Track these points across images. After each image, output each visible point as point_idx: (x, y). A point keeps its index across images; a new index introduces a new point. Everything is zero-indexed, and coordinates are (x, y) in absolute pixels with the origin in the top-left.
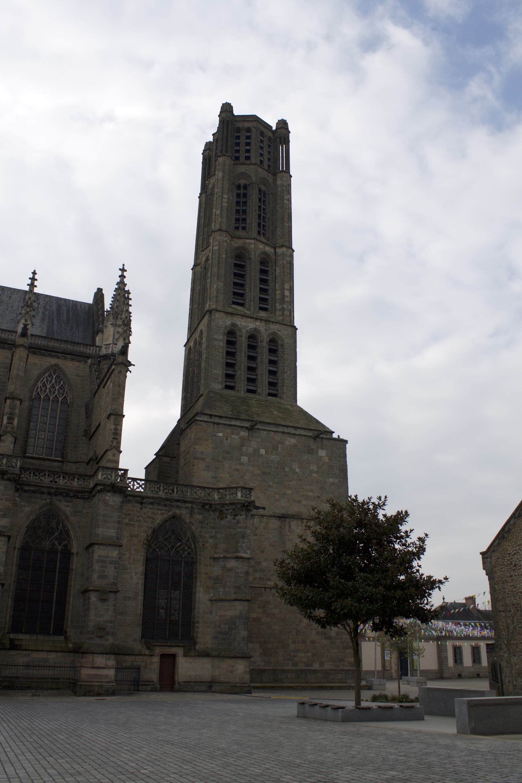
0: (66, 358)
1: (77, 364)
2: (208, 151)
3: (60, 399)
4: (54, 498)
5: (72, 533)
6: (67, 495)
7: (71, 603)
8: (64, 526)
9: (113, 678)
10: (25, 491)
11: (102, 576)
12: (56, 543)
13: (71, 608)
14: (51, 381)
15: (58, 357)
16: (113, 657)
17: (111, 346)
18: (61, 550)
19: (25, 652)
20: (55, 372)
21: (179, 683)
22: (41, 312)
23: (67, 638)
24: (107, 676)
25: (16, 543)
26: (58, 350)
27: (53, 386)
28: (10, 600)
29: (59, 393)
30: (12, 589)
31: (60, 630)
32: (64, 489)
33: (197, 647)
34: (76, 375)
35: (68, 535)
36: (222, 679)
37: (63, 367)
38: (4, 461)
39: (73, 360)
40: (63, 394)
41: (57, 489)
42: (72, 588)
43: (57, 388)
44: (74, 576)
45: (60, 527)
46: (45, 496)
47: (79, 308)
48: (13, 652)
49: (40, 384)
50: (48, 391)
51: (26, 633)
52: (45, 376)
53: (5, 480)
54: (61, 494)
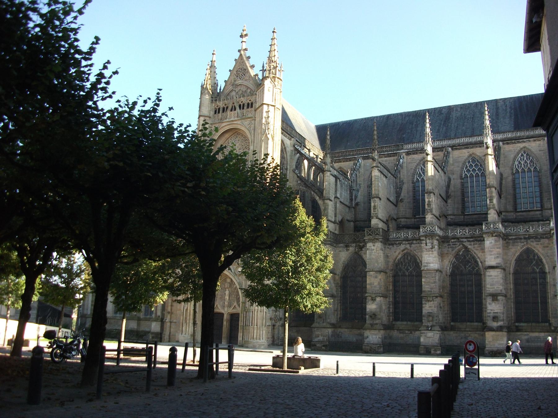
0: (529, 141)
1: (538, 142)
3: (532, 169)
4: (529, 241)
5: (544, 260)
6: (536, 238)
7: (550, 302)
8: (538, 257)
10: (510, 239)
12: (535, 267)
13: (550, 306)
14: (523, 159)
15: (525, 142)
18: (539, 271)
19: (525, 333)
20: (525, 153)
22: (508, 112)
23: (550, 324)
25: (510, 271)
26: (523, 138)
27: (526, 162)
28: (512, 304)
29: (531, 166)
30: (512, 297)
31: (546, 320)
32: (534, 234)
34: (540, 151)
35: (542, 262)
37: (530, 147)
38: (492, 226)
39: (535, 141)
40: (533, 165)
41: (529, 235)
42: (549, 294)
43: (528, 162)
44: (549, 287)
45: (536, 257)
46: (523, 240)
47: (534, 99)
48: (519, 333)
49: (516, 163)
50: (523, 166)
51: (525, 322)
52: (518, 157)
53: (495, 236)
54: (532, 238)
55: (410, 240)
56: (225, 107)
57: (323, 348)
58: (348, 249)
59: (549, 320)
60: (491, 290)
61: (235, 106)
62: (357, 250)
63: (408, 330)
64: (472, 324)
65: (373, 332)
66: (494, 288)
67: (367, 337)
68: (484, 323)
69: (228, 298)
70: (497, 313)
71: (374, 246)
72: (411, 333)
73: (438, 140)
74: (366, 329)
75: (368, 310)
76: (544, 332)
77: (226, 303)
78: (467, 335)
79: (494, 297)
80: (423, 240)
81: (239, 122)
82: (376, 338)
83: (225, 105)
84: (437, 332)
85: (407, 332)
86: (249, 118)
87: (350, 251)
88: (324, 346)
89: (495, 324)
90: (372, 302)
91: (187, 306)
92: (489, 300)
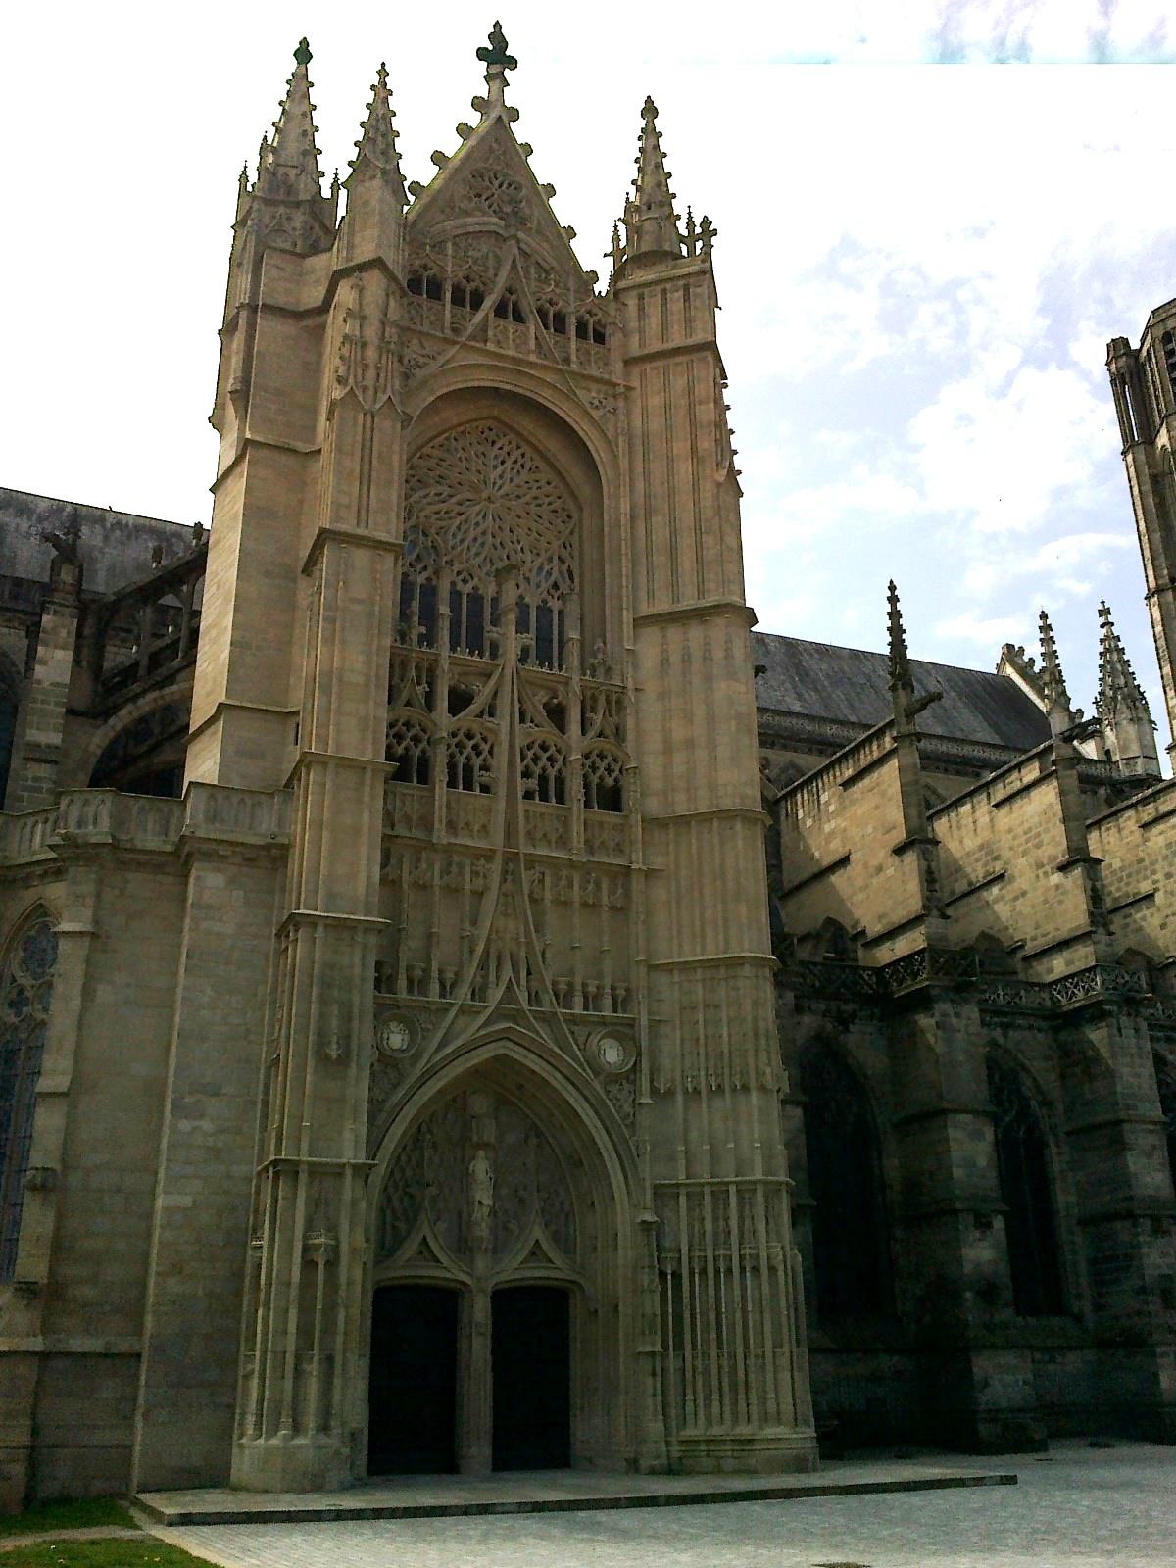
2: (1124, 359)
17: (1139, 760)
55: (1006, 1014)
61: (515, 304)
69: (488, 1202)
71: (956, 1015)
72: (1052, 1360)
75: (968, 1269)
77: (483, 1230)
80: (1110, 1014)
83: (468, 279)
90: (978, 1234)
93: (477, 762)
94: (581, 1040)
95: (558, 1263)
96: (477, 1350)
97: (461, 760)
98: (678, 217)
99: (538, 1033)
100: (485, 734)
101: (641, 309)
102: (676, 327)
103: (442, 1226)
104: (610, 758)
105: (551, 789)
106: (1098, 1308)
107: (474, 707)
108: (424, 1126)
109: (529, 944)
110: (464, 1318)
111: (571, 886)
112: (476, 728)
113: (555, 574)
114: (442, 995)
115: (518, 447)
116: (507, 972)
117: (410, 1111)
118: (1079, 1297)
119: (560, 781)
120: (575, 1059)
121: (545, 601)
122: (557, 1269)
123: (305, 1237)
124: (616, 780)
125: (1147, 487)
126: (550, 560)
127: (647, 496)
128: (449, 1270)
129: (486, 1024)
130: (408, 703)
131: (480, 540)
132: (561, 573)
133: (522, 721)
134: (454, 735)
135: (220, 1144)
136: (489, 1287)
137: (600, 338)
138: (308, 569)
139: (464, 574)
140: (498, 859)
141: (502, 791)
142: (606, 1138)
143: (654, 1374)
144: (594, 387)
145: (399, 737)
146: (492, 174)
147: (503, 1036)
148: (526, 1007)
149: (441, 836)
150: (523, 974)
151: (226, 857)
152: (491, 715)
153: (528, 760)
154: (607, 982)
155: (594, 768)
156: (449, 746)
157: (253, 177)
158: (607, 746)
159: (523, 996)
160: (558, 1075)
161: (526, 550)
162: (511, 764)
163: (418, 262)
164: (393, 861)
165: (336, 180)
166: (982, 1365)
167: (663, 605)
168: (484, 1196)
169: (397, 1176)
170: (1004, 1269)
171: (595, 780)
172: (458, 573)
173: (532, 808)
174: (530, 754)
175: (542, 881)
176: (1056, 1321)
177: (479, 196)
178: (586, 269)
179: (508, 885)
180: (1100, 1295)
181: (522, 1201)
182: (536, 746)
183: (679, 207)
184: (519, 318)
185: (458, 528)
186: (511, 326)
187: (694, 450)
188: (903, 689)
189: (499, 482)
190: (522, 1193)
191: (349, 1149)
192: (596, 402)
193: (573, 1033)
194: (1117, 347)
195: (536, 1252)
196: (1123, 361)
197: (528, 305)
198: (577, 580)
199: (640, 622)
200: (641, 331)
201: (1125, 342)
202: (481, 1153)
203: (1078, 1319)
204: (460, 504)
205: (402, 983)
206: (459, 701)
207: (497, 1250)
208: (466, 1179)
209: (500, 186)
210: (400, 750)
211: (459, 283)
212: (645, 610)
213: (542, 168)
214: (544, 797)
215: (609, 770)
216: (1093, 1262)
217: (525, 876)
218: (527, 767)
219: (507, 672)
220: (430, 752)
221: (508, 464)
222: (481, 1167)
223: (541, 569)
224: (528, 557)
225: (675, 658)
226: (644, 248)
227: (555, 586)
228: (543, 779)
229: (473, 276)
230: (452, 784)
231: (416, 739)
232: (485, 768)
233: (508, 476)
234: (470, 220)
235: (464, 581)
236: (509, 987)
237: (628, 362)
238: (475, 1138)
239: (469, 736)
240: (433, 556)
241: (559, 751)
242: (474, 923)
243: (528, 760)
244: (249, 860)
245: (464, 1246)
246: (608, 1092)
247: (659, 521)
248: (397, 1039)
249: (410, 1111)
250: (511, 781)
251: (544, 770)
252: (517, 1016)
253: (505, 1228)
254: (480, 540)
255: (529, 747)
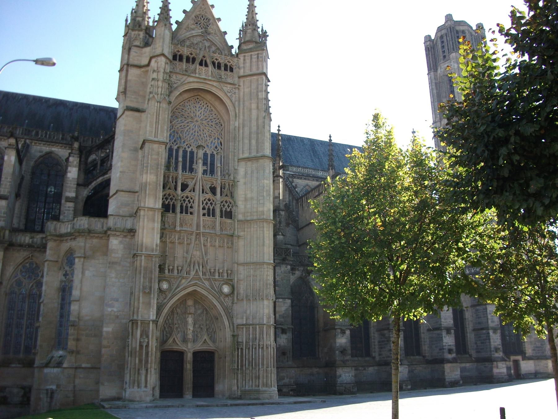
7: (469, 337)
9: (506, 374)
11: (493, 322)
13: (469, 339)
16: (504, 362)
21: (523, 375)
23: (471, 356)
24: (504, 373)
33: (527, 355)
36: (541, 371)
42: (468, 329)
56: (191, 56)
57: (291, 393)
58: (294, 272)
59: (468, 353)
60: (445, 324)
61: (206, 61)
62: (304, 274)
63: (362, 366)
64: (414, 357)
65: (345, 369)
66: (447, 322)
67: (340, 376)
68: (424, 357)
69: (192, 329)
70: (450, 345)
72: (365, 369)
73: (322, 171)
74: (339, 367)
75: (338, 345)
76: (469, 363)
77: (190, 336)
78: (414, 368)
79: (448, 331)
81: (215, 84)
82: (349, 376)
84: (406, 366)
85: (360, 368)
86: (230, 84)
87: (296, 275)
88: (291, 390)
89: (450, 356)
90: (342, 335)
91: (146, 340)
92: (444, 333)
93: (189, 205)
94: (217, 286)
95: (211, 345)
96: (189, 367)
97: (184, 205)
98: (259, 28)
99: (204, 284)
100: (192, 197)
101: (244, 60)
102: (254, 67)
103: (179, 335)
104: (229, 202)
105: (210, 213)
106: (380, 355)
107: (189, 189)
108: (174, 309)
109: (203, 258)
110: (185, 359)
111: (216, 241)
112: (189, 195)
113: (216, 143)
114: (178, 273)
115: (206, 104)
116: (197, 267)
117: (169, 305)
118: (375, 352)
119: (213, 210)
120: (215, 291)
121: (213, 152)
122: (211, 346)
123: (140, 339)
124: (231, 209)
125: (434, 87)
126: (215, 139)
127: (243, 120)
128: (181, 347)
129: (189, 282)
130: (169, 189)
131: (194, 134)
132: (218, 143)
133: (203, 193)
134: (182, 197)
135: (119, 314)
136: (192, 351)
137: (232, 70)
138: (142, 148)
139: (189, 145)
140: (194, 234)
141: (196, 214)
142: (224, 313)
143: (235, 374)
144: (229, 86)
145: (167, 199)
146: (201, 16)
147: (195, 285)
148: (202, 277)
149: (178, 228)
150: (201, 267)
151: (118, 235)
152: (194, 191)
153: (204, 204)
154: (225, 269)
155: (224, 206)
156: (181, 201)
157: (129, 22)
158: (229, 199)
159: (201, 274)
160: (211, 296)
161: (208, 136)
162: (199, 206)
163: (176, 50)
164: (164, 236)
165: (154, 19)
166: (340, 371)
167: (246, 155)
168: (191, 328)
169: (167, 322)
170: (349, 345)
171: (224, 209)
172: (187, 145)
173: (205, 219)
174: (205, 202)
175: (207, 240)
176: (368, 359)
177: (197, 23)
178: (230, 44)
179: (197, 242)
180: (380, 351)
181: (201, 328)
182: (207, 200)
183: (259, 24)
184: (206, 65)
185: (187, 131)
186: (203, 68)
187: (258, 108)
188: (332, 169)
189: (200, 115)
190: (202, 326)
191: (153, 316)
192: (229, 91)
193: (215, 283)
194: (427, 39)
195: (205, 341)
196: (428, 43)
197: (209, 62)
198: (223, 145)
199: (240, 160)
200: (244, 67)
201: (429, 36)
202: (190, 316)
203: (374, 358)
204: (188, 123)
205: (167, 271)
206: (184, 187)
207: (194, 341)
208: (186, 323)
209: (204, 19)
210: (167, 203)
211: (188, 56)
212: (241, 156)
213: (216, 13)
214: (209, 215)
215: (228, 206)
216: (379, 342)
217: (202, 239)
218: (204, 206)
219: (198, 179)
220: (175, 203)
221: (203, 109)
222: (190, 320)
223: (212, 142)
224: (208, 138)
225: (249, 172)
226: (247, 39)
227: (216, 147)
228: (209, 209)
229: (193, 53)
230: (181, 212)
231: (171, 199)
232: (191, 207)
233: (202, 113)
234: (193, 32)
235: (189, 147)
236: (197, 271)
237: (239, 77)
238: (188, 312)
239: (187, 197)
240: (179, 140)
241: (213, 201)
242: (187, 253)
243: (204, 204)
244: (125, 236)
245: (185, 340)
246: (224, 300)
247: (247, 129)
248: (165, 286)
249: (169, 305)
250: (199, 211)
251: (209, 207)
252: (199, 279)
253: (197, 336)
254: (194, 134)
255: (205, 200)
